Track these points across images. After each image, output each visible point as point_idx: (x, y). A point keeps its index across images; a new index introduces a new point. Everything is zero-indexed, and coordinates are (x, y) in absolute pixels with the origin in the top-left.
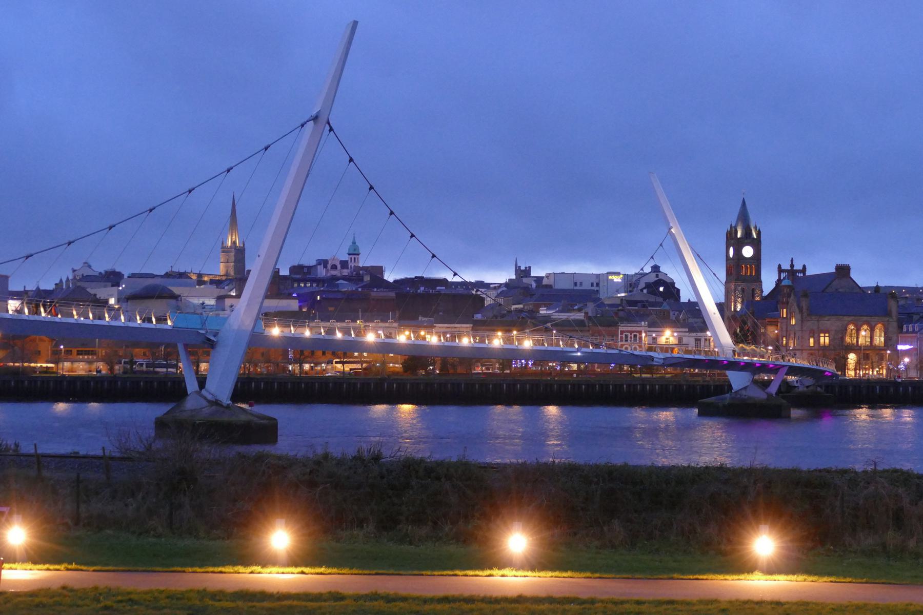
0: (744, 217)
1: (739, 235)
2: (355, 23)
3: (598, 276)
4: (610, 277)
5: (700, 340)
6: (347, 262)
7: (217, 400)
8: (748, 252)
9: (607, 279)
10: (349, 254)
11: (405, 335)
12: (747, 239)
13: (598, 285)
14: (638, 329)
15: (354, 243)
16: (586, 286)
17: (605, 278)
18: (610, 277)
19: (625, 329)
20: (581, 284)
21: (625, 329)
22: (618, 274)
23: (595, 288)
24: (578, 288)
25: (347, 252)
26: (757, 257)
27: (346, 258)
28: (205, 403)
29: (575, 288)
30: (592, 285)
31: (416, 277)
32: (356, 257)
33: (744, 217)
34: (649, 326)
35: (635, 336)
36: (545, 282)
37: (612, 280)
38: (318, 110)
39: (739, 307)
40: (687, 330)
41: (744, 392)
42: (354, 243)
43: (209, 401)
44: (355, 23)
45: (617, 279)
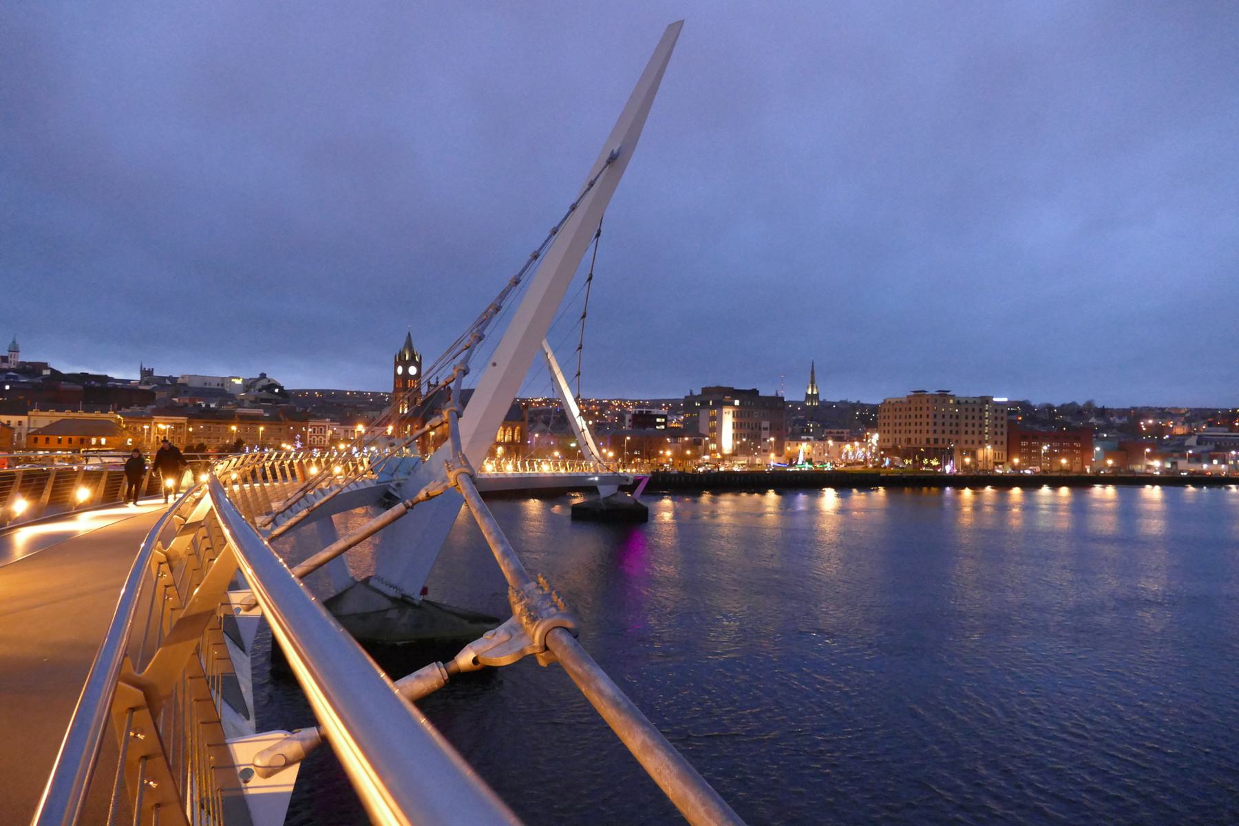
0: (409, 345)
1: (407, 358)
2: (675, 29)
3: (223, 379)
4: (233, 380)
5: (348, 431)
6: (7, 357)
7: (404, 596)
8: (413, 370)
9: (231, 382)
10: (10, 351)
11: (346, 446)
12: (412, 361)
13: (222, 385)
14: (324, 424)
15: (14, 342)
16: (214, 386)
17: (229, 380)
18: (233, 380)
19: (314, 424)
20: (210, 384)
21: (314, 424)
22: (239, 378)
23: (220, 387)
24: (207, 386)
25: (7, 349)
26: (418, 375)
27: (6, 354)
28: (386, 604)
29: (206, 387)
30: (218, 385)
31: (81, 373)
32: (16, 353)
33: (409, 345)
34: (331, 421)
35: (321, 429)
36: (179, 381)
37: (234, 382)
38: (619, 146)
39: (406, 411)
40: (339, 423)
41: (613, 499)
42: (14, 342)
43: (393, 600)
44: (675, 29)
45: (238, 382)
